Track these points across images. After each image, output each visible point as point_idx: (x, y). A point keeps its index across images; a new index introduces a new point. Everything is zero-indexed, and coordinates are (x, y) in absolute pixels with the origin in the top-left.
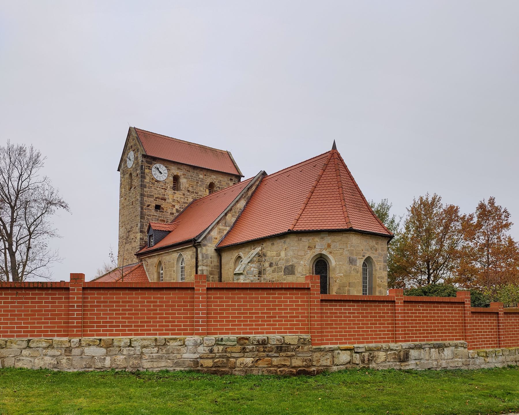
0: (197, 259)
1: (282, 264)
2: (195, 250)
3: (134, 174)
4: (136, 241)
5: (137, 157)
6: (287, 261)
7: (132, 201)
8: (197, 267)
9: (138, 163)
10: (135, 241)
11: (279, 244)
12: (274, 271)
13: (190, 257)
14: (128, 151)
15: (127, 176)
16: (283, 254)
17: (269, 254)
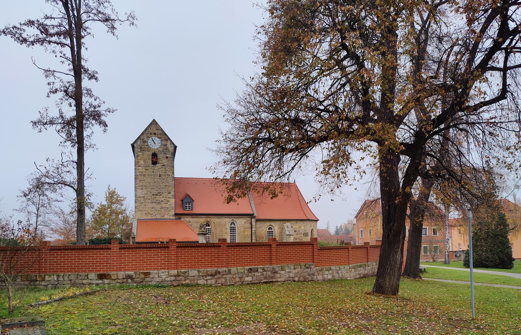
0: (251, 224)
1: (302, 232)
2: (250, 219)
3: (160, 156)
4: (169, 203)
5: (166, 145)
6: (305, 231)
7: (158, 173)
8: (252, 228)
9: (167, 149)
10: (167, 203)
11: (300, 224)
12: (297, 234)
13: (243, 223)
14: (149, 135)
15: (150, 153)
16: (303, 228)
17: (294, 226)
